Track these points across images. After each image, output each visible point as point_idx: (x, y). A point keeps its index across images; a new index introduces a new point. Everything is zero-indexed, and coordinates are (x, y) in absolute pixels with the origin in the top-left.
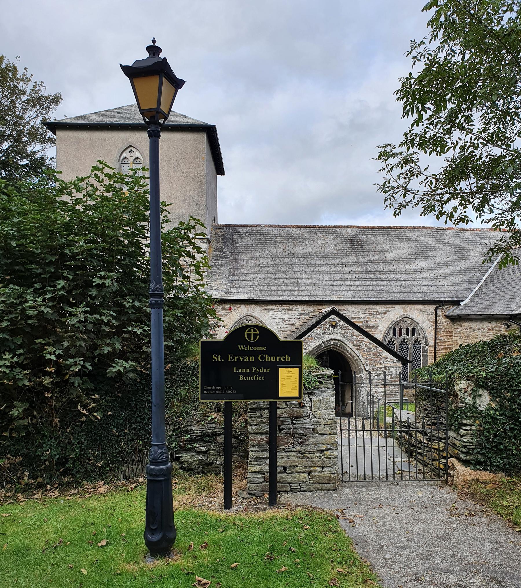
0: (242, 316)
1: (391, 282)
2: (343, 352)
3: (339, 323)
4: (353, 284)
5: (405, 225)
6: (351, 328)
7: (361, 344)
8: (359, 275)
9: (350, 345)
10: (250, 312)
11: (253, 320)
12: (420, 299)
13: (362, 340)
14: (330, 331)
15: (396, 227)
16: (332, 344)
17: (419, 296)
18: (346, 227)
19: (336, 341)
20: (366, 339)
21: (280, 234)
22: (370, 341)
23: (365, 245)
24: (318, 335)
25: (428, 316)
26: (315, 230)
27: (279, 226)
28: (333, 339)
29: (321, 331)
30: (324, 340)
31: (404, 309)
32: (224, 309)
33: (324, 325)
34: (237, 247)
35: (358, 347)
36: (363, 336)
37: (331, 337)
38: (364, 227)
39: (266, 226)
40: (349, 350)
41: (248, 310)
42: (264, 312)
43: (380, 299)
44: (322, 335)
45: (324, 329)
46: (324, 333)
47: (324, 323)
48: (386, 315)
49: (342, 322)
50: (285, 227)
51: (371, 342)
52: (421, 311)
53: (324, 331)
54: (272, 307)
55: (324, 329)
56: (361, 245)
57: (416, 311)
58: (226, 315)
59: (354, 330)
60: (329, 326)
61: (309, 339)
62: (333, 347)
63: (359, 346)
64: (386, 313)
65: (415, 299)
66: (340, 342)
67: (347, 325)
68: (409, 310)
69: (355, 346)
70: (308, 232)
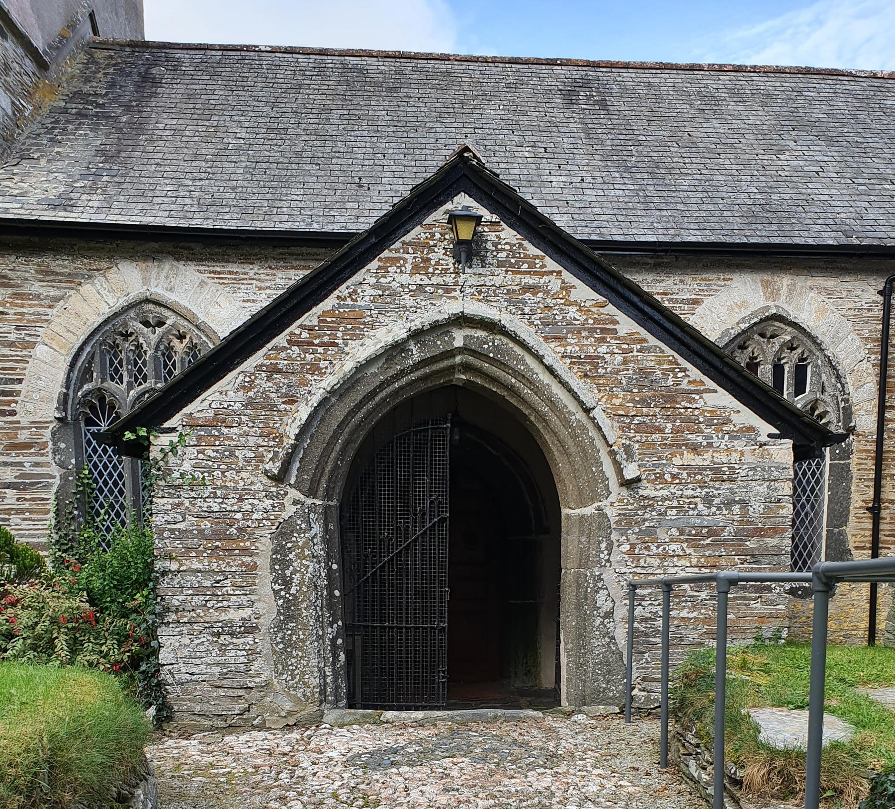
0: (122, 302)
1: (716, 194)
2: (511, 389)
3: (492, 236)
4: (571, 198)
5: (749, 62)
6: (551, 264)
7: (603, 349)
8: (597, 174)
9: (551, 352)
10: (158, 290)
11: (171, 319)
12: (831, 242)
13: (606, 331)
14: (449, 279)
15: (720, 66)
16: (459, 343)
17: (826, 235)
18: (552, 62)
19: (481, 334)
20: (627, 325)
21: (321, 71)
22: (644, 333)
23: (618, 104)
24: (387, 297)
25: (855, 317)
26: (443, 67)
27: (322, 52)
28: (462, 320)
29: (405, 279)
30: (417, 324)
31: (766, 285)
32: (46, 273)
33: (417, 245)
34: (154, 95)
35: (589, 365)
36: (611, 309)
37: (450, 307)
38: (612, 66)
39: (274, 50)
40: (545, 378)
41: (146, 281)
42: (212, 285)
43: (678, 239)
44: (409, 301)
45: (416, 270)
46: (420, 288)
47: (416, 233)
48: (699, 309)
49: (509, 235)
50: (342, 54)
51: (653, 341)
52: (830, 294)
53: (417, 278)
54: (247, 268)
55: (416, 270)
56: (603, 104)
57: (813, 294)
58: (57, 299)
59: (567, 276)
60: (440, 255)
61: (342, 319)
62: (466, 367)
63: (594, 360)
64: (696, 302)
65: (811, 242)
66: (499, 340)
67: (533, 250)
68: (784, 290)
69: (576, 360)
70: (415, 70)
